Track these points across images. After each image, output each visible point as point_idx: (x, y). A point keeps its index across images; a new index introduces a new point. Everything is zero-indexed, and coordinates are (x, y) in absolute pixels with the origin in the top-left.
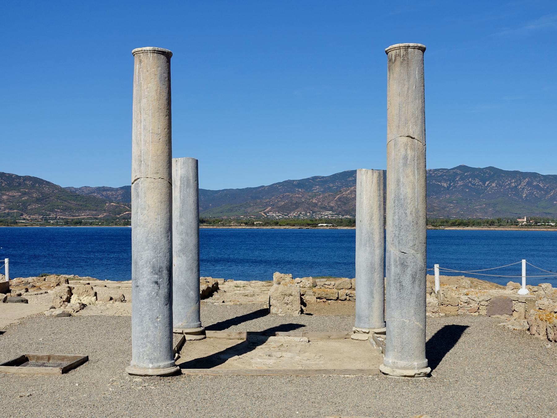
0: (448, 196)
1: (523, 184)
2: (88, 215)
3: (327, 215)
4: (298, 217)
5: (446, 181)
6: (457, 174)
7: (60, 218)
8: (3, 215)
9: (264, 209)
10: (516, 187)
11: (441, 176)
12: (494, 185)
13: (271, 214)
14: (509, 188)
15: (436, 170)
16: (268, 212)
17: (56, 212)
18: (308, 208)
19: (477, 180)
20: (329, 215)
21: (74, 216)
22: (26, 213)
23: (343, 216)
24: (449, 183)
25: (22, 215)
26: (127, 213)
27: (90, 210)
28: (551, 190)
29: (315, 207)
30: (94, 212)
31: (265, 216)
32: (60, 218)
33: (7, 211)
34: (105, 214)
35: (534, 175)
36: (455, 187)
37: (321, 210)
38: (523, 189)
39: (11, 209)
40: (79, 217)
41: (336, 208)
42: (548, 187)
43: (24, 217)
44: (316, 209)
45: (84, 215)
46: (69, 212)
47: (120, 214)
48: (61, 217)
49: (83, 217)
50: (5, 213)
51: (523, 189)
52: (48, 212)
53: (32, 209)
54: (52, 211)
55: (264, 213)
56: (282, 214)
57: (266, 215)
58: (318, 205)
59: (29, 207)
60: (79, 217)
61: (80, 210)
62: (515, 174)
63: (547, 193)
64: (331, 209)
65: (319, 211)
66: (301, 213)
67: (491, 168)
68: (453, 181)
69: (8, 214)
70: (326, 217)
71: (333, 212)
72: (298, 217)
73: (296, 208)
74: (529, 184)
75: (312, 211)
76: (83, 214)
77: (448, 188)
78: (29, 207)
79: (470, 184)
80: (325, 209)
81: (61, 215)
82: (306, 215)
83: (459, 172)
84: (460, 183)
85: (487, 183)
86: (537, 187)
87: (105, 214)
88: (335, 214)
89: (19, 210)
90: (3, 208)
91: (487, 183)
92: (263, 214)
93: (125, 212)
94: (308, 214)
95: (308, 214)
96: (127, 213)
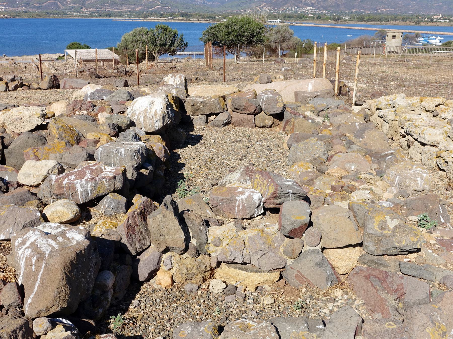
2: (128, 9)
3: (307, 10)
4: (285, 11)
7: (108, 10)
8: (68, 8)
9: (259, 5)
13: (264, 9)
16: (263, 7)
17: (106, 5)
18: (294, 4)
20: (309, 10)
21: (118, 9)
22: (85, 7)
23: (320, 11)
25: (82, 8)
26: (157, 7)
27: (130, 5)
29: (300, 3)
30: (133, 6)
31: (260, 10)
32: (108, 10)
33: (71, 5)
34: (141, 8)
37: (304, 6)
39: (74, 3)
40: (122, 10)
41: (316, 4)
43: (83, 10)
44: (300, 5)
45: (126, 9)
46: (115, 6)
47: (152, 8)
48: (109, 10)
49: (124, 10)
50: (70, 7)
52: (100, 6)
53: (89, 4)
54: (103, 5)
55: (260, 8)
56: (273, 9)
57: (261, 9)
58: (302, 2)
59: (87, 2)
60: (122, 10)
61: (123, 4)
64: (312, 5)
65: (302, 7)
66: (288, 9)
69: (72, 7)
70: (307, 11)
71: (313, 7)
72: (285, 11)
73: (285, 4)
75: (296, 6)
76: (125, 8)
78: (87, 2)
80: (307, 5)
81: (109, 9)
82: (292, 9)
87: (141, 8)
88: (314, 9)
89: (79, 4)
90: (69, 2)
92: (259, 9)
93: (156, 6)
94: (293, 9)
95: (293, 9)
96: (157, 7)
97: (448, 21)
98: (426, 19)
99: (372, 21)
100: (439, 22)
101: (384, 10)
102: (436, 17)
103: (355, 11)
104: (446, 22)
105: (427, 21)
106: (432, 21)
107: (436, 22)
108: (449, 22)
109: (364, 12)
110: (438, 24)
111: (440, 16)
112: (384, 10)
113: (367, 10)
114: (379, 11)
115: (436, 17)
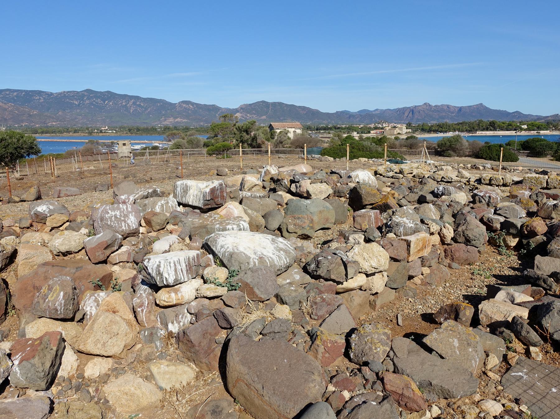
0: (78, 111)
1: (131, 103)
5: (77, 100)
6: (85, 96)
10: (126, 105)
11: (73, 96)
12: (111, 103)
14: (121, 106)
15: (69, 92)
19: (99, 100)
24: (79, 101)
28: (148, 108)
35: (137, 98)
36: (84, 104)
38: (131, 106)
42: (146, 106)
51: (131, 106)
62: (125, 96)
63: (146, 109)
67: (109, 92)
68: (82, 100)
74: (134, 103)
77: (79, 105)
79: (94, 103)
83: (86, 94)
84: (87, 102)
85: (106, 102)
86: (140, 105)
91: (106, 102)
97: (114, 131)
98: (96, 131)
99: (46, 133)
100: (107, 132)
101: (54, 123)
102: (103, 129)
103: (25, 125)
104: (113, 132)
105: (97, 132)
106: (101, 132)
107: (105, 132)
108: (116, 133)
109: (33, 126)
110: (108, 134)
111: (107, 128)
112: (54, 123)
113: (37, 124)
114: (49, 124)
115: (103, 129)
